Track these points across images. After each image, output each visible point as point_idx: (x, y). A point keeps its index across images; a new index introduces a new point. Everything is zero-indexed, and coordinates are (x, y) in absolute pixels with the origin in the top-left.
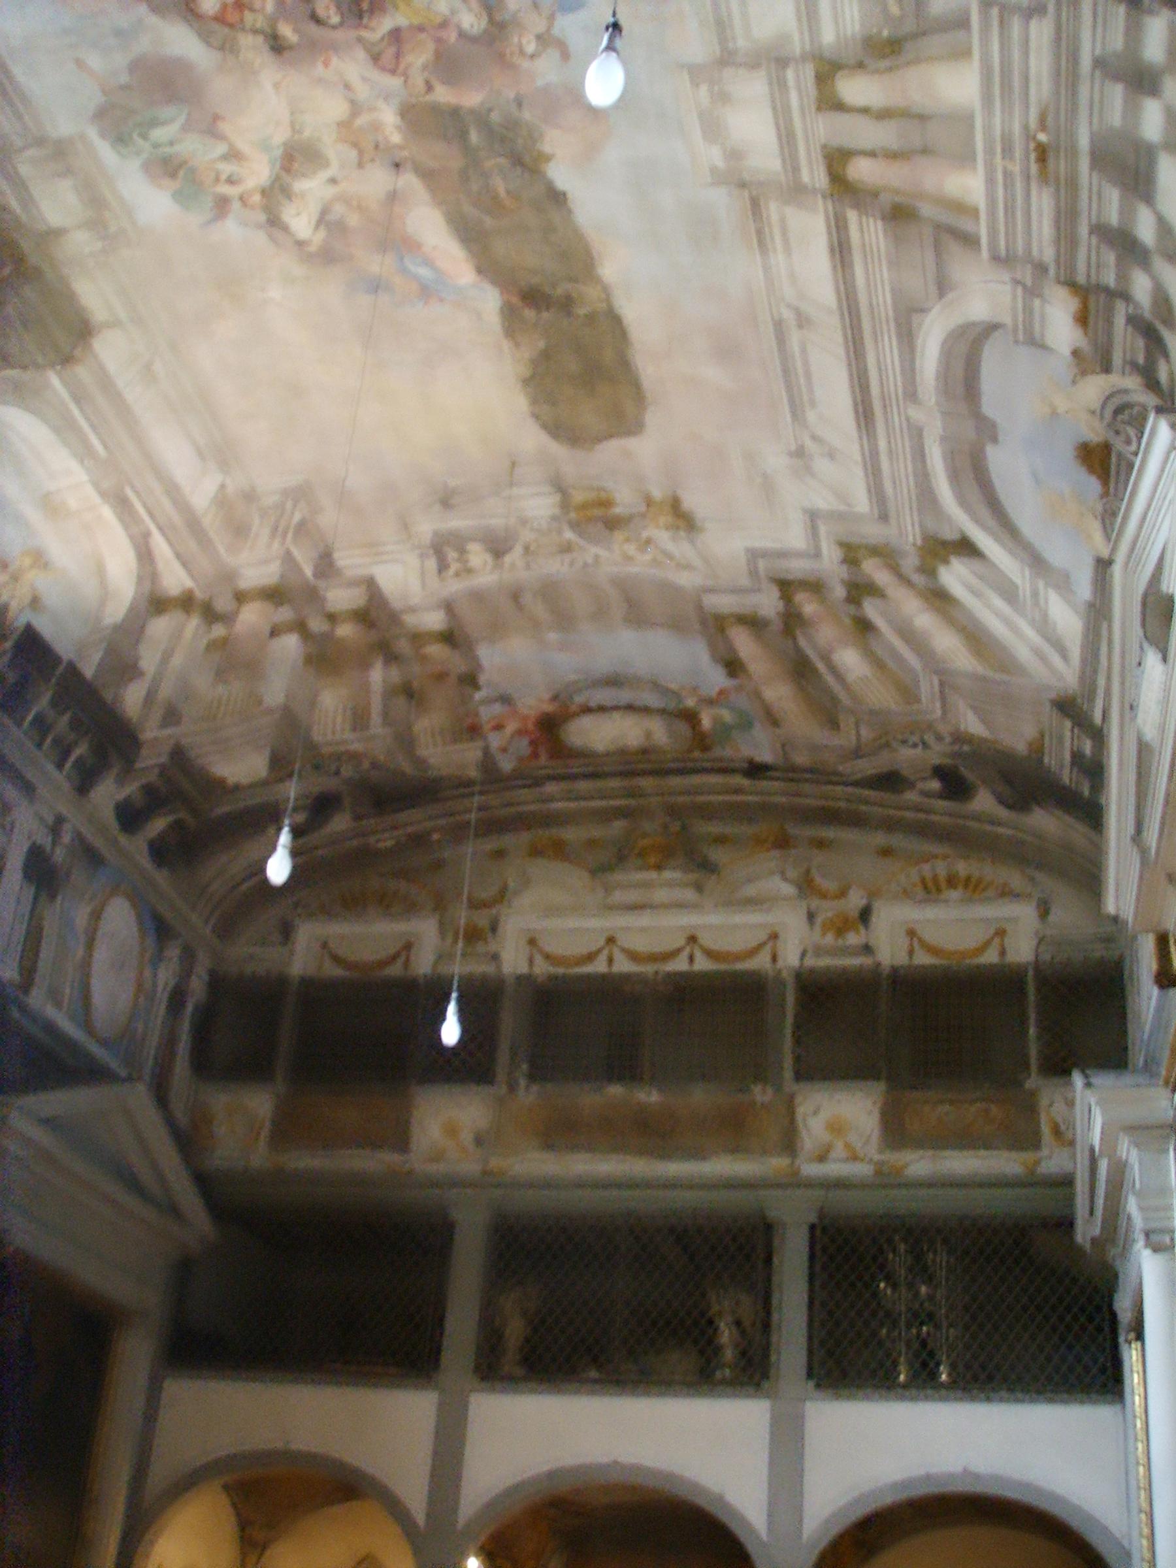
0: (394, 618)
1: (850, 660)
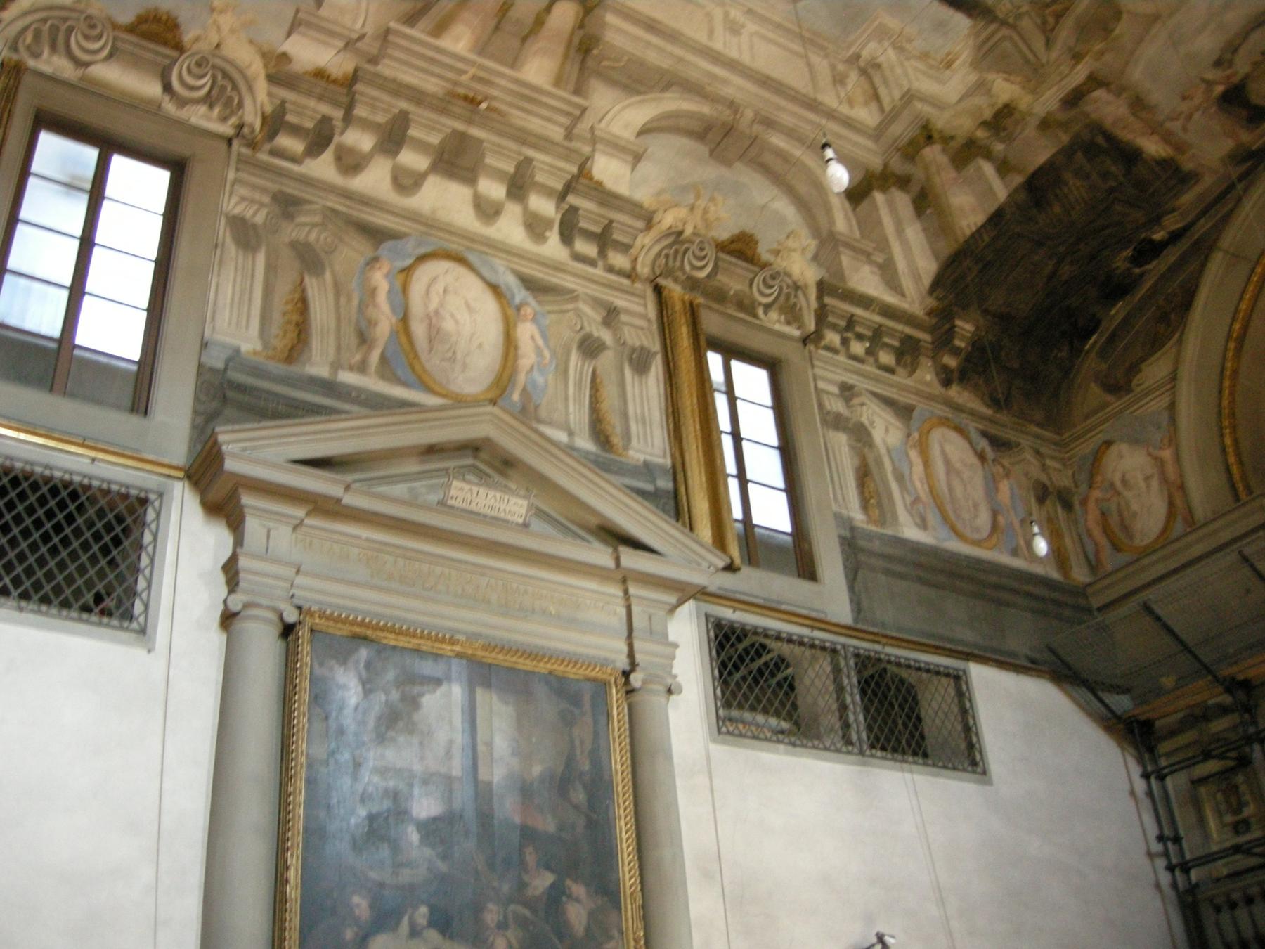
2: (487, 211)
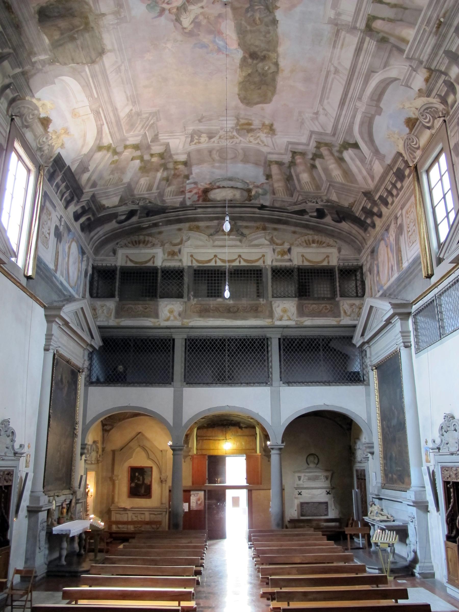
0: (171, 156)
1: (305, 177)
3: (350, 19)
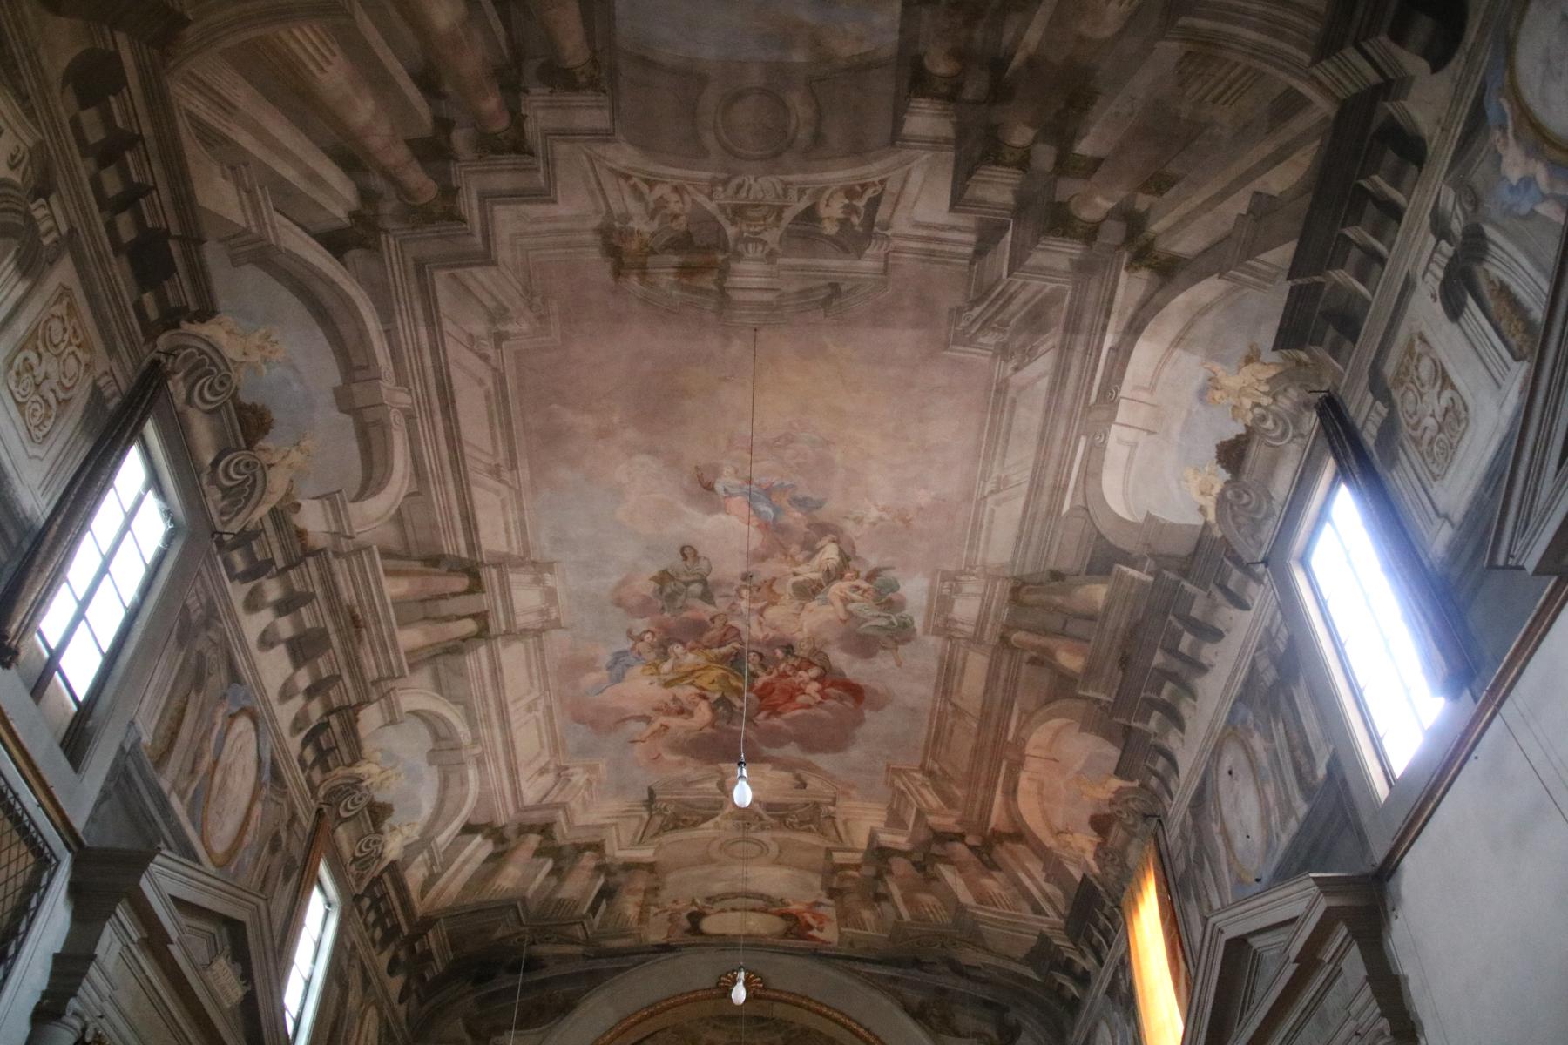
2: (286, 693)
3: (512, 577)
